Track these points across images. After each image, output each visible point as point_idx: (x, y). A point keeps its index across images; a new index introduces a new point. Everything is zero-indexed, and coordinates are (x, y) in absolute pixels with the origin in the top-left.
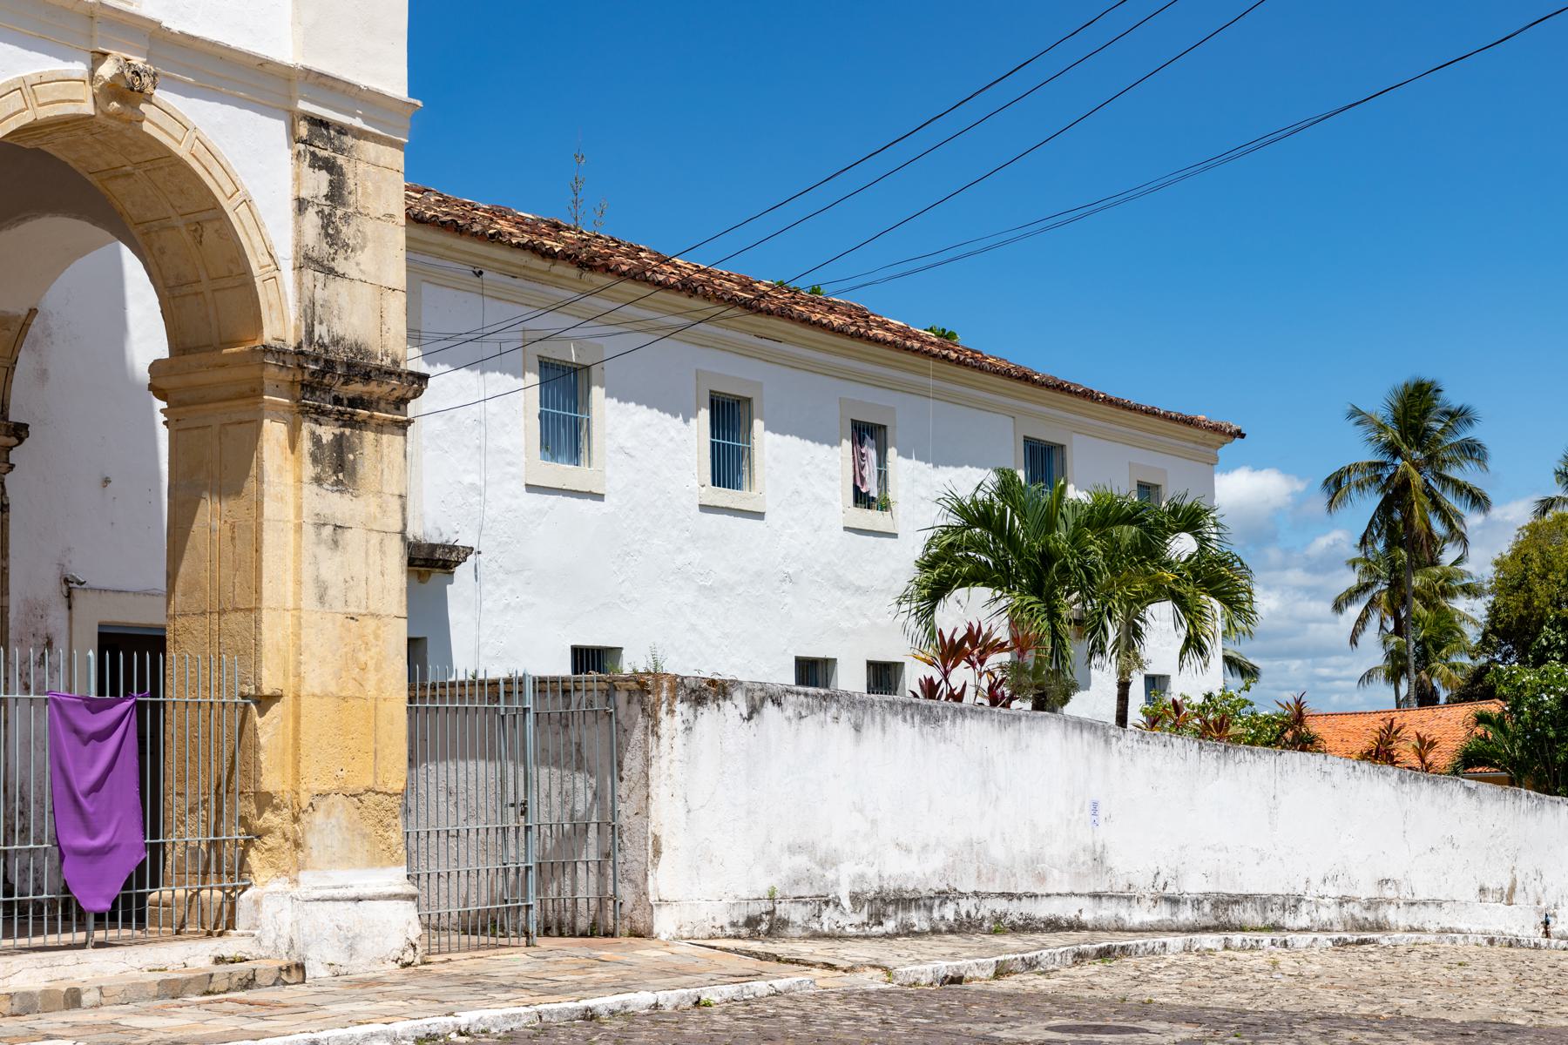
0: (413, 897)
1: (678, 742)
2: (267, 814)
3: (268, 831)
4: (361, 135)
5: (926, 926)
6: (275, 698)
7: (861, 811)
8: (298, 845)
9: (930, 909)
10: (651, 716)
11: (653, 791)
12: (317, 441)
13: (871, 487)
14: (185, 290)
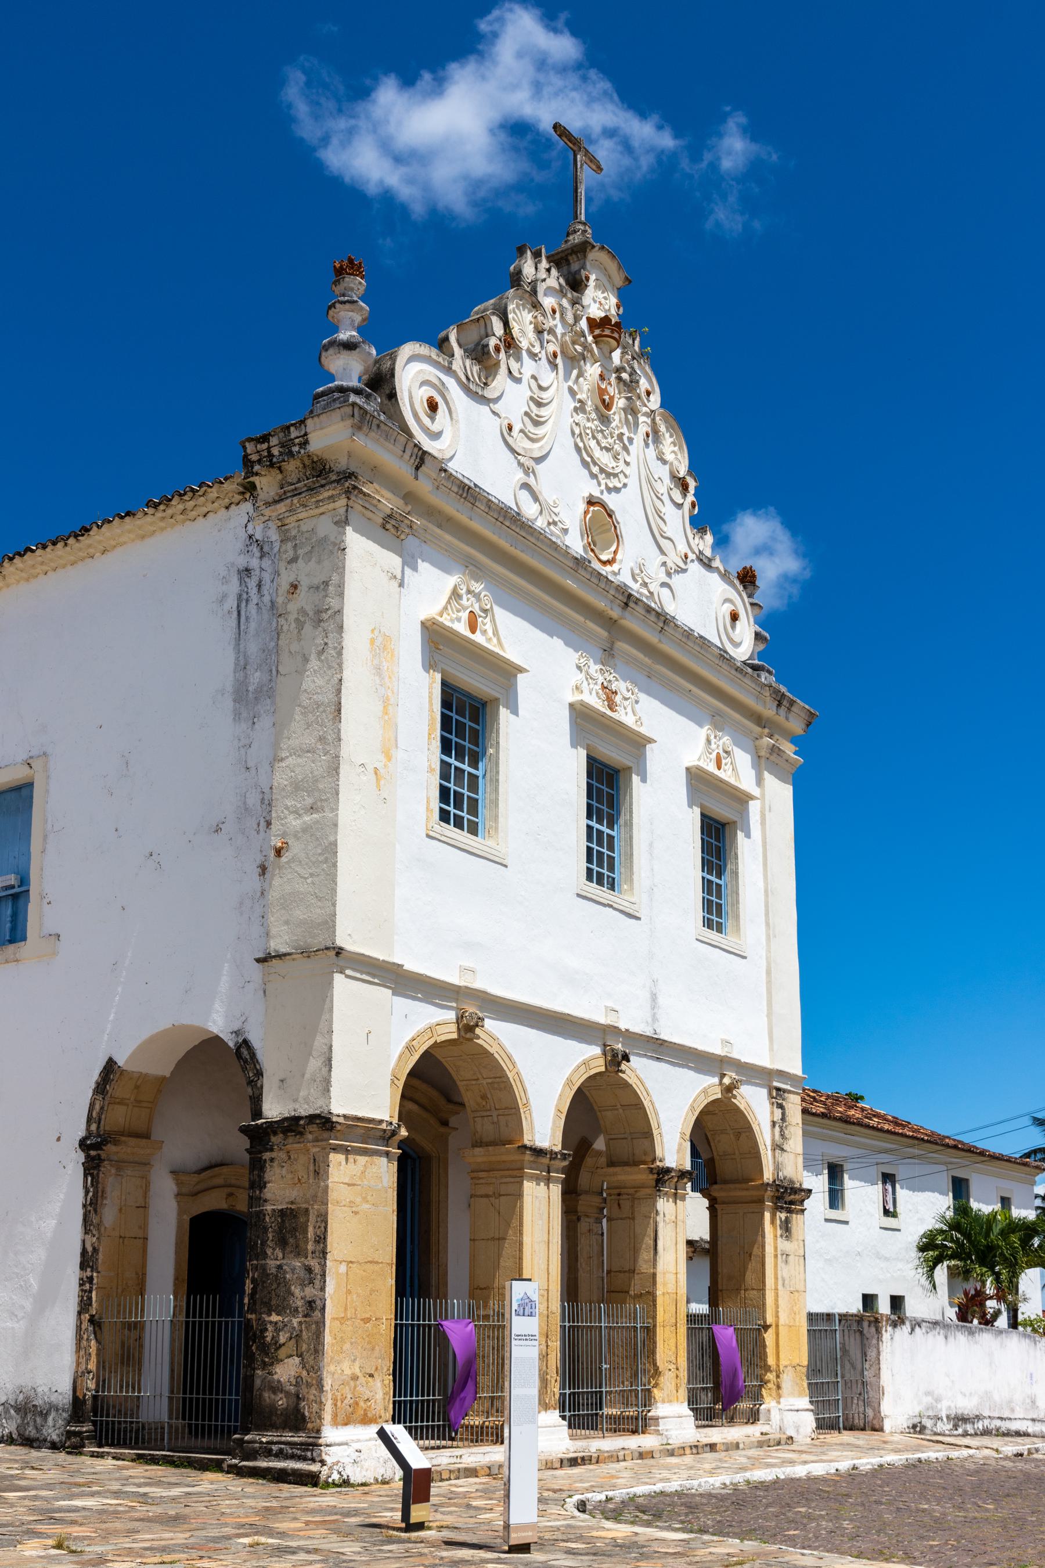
0: (812, 1411)
1: (889, 1344)
2: (768, 1374)
3: (769, 1381)
4: (790, 1092)
5: (972, 1432)
6: (770, 1326)
7: (948, 1376)
8: (779, 1387)
9: (974, 1423)
10: (878, 1331)
11: (881, 1366)
12: (781, 1219)
13: (890, 1207)
14: (727, 1157)
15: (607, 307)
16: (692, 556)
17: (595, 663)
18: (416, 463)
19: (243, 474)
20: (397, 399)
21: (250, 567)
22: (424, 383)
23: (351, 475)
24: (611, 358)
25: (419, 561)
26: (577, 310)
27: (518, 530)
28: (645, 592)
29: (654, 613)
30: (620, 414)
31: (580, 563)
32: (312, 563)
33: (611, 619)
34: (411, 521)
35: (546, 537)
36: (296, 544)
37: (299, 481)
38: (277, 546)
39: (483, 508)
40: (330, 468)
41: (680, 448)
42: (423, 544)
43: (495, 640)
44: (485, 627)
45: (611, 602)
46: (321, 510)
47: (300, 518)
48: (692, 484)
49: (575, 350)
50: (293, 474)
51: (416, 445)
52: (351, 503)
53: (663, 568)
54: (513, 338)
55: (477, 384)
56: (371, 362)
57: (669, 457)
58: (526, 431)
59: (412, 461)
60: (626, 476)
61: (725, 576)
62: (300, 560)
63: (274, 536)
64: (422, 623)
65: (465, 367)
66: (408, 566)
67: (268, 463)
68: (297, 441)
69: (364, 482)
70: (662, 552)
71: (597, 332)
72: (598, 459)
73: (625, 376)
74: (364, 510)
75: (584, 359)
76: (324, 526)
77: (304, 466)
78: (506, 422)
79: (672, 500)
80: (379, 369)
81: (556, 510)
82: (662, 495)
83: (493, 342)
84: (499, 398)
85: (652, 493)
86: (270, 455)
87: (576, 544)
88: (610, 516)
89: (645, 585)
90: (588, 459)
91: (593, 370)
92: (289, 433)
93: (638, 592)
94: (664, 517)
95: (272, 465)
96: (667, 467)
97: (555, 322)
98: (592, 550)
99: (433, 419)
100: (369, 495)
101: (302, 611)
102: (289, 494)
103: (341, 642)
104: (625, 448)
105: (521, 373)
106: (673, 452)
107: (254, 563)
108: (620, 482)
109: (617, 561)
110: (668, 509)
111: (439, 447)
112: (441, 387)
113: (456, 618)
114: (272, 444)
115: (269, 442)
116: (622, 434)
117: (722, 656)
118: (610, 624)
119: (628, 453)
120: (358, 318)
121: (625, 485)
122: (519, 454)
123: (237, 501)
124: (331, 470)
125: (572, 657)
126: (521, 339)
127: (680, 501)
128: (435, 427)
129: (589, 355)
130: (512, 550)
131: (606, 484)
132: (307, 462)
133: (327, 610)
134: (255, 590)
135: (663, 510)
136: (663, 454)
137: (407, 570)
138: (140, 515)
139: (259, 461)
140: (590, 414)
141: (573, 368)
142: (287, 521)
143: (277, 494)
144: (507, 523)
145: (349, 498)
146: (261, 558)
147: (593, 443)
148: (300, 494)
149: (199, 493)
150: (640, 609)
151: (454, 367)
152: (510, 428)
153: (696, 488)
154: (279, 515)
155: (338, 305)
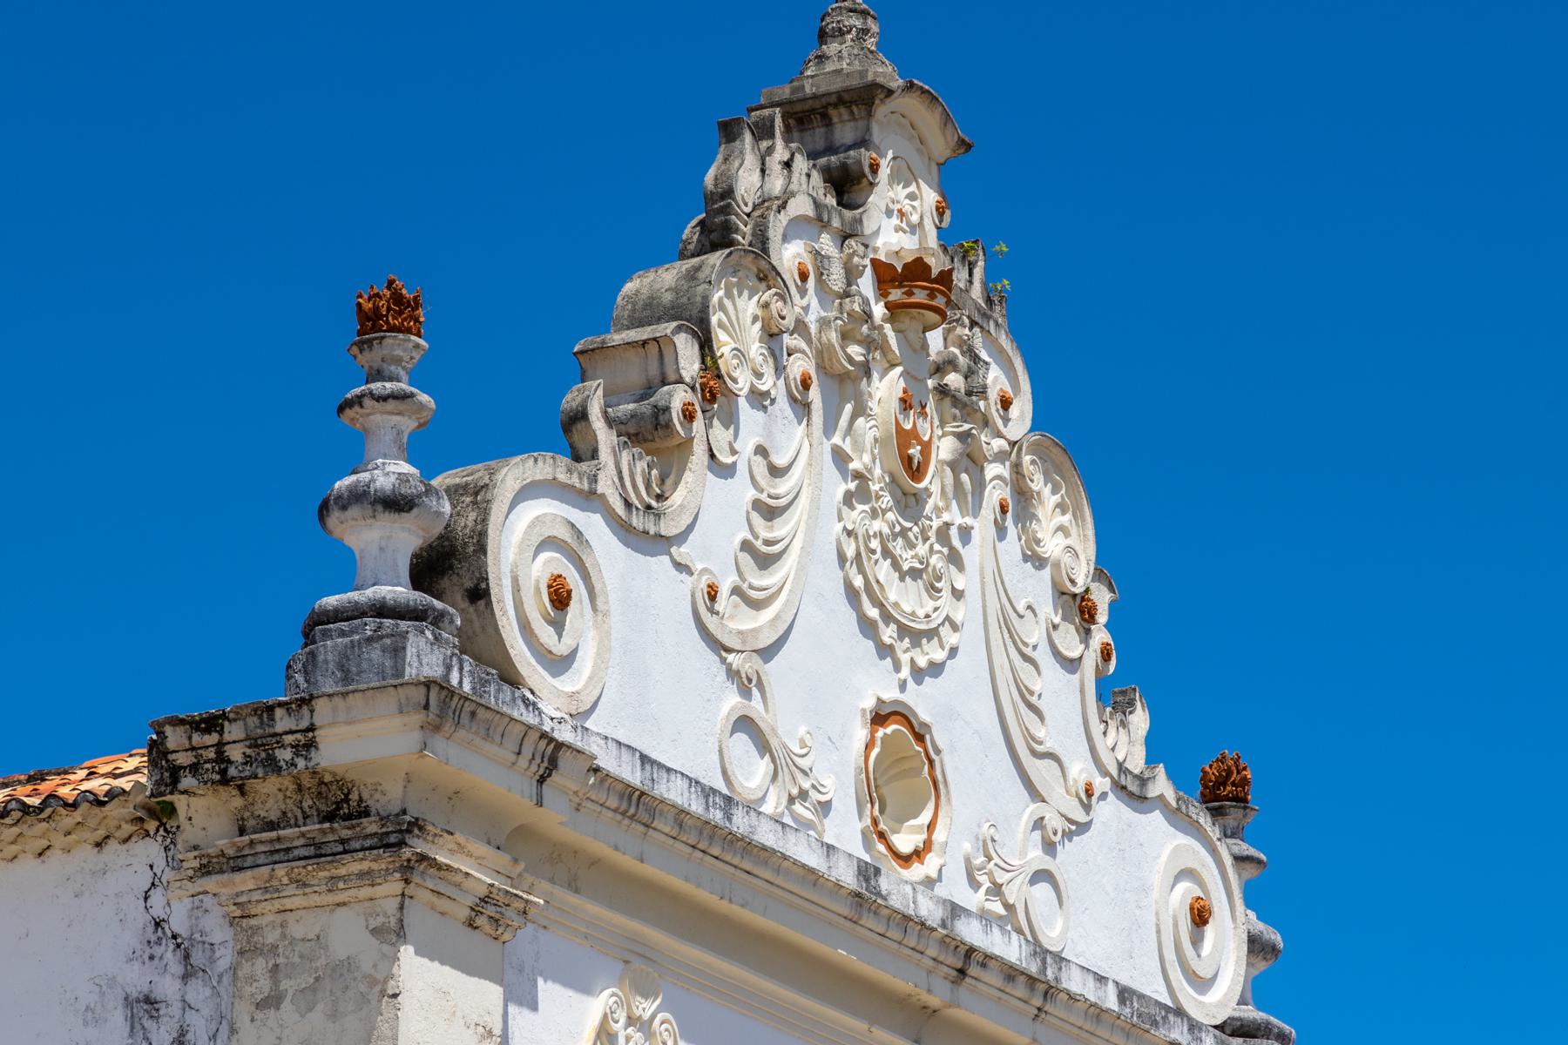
15: (915, 218)
18: (541, 772)
20: (489, 604)
21: (157, 994)
26: (851, 256)
29: (1022, 979)
32: (317, 1017)
33: (924, 1007)
34: (527, 901)
36: (276, 966)
38: (225, 958)
40: (361, 800)
42: (542, 931)
45: (929, 972)
46: (341, 897)
48: (1102, 598)
49: (850, 360)
53: (1037, 835)
54: (719, 376)
57: (1052, 546)
58: (745, 586)
60: (955, 627)
62: (286, 1004)
63: (218, 930)
65: (620, 473)
68: (289, 739)
69: (435, 835)
70: (1035, 794)
71: (896, 295)
72: (896, 605)
73: (954, 380)
75: (868, 374)
77: (300, 788)
79: (1056, 653)
81: (804, 763)
82: (1035, 647)
83: (679, 398)
85: (1012, 650)
86: (222, 759)
88: (920, 738)
90: (873, 613)
91: (886, 388)
94: (1041, 704)
96: (1046, 573)
97: (804, 302)
98: (882, 836)
99: (558, 626)
100: (449, 868)
104: (955, 559)
105: (734, 452)
106: (1061, 529)
107: (168, 987)
109: (935, 847)
111: (569, 689)
114: (227, 737)
121: (953, 652)
123: (126, 836)
127: (1074, 654)
128: (561, 648)
130: (723, 906)
131: (912, 661)
132: (307, 781)
135: (1037, 687)
136: (1038, 542)
140: (878, 498)
141: (844, 401)
143: (234, 844)
145: (407, 881)
146: (185, 977)
147: (884, 571)
150: (992, 977)
152: (712, 594)
153: (1112, 604)
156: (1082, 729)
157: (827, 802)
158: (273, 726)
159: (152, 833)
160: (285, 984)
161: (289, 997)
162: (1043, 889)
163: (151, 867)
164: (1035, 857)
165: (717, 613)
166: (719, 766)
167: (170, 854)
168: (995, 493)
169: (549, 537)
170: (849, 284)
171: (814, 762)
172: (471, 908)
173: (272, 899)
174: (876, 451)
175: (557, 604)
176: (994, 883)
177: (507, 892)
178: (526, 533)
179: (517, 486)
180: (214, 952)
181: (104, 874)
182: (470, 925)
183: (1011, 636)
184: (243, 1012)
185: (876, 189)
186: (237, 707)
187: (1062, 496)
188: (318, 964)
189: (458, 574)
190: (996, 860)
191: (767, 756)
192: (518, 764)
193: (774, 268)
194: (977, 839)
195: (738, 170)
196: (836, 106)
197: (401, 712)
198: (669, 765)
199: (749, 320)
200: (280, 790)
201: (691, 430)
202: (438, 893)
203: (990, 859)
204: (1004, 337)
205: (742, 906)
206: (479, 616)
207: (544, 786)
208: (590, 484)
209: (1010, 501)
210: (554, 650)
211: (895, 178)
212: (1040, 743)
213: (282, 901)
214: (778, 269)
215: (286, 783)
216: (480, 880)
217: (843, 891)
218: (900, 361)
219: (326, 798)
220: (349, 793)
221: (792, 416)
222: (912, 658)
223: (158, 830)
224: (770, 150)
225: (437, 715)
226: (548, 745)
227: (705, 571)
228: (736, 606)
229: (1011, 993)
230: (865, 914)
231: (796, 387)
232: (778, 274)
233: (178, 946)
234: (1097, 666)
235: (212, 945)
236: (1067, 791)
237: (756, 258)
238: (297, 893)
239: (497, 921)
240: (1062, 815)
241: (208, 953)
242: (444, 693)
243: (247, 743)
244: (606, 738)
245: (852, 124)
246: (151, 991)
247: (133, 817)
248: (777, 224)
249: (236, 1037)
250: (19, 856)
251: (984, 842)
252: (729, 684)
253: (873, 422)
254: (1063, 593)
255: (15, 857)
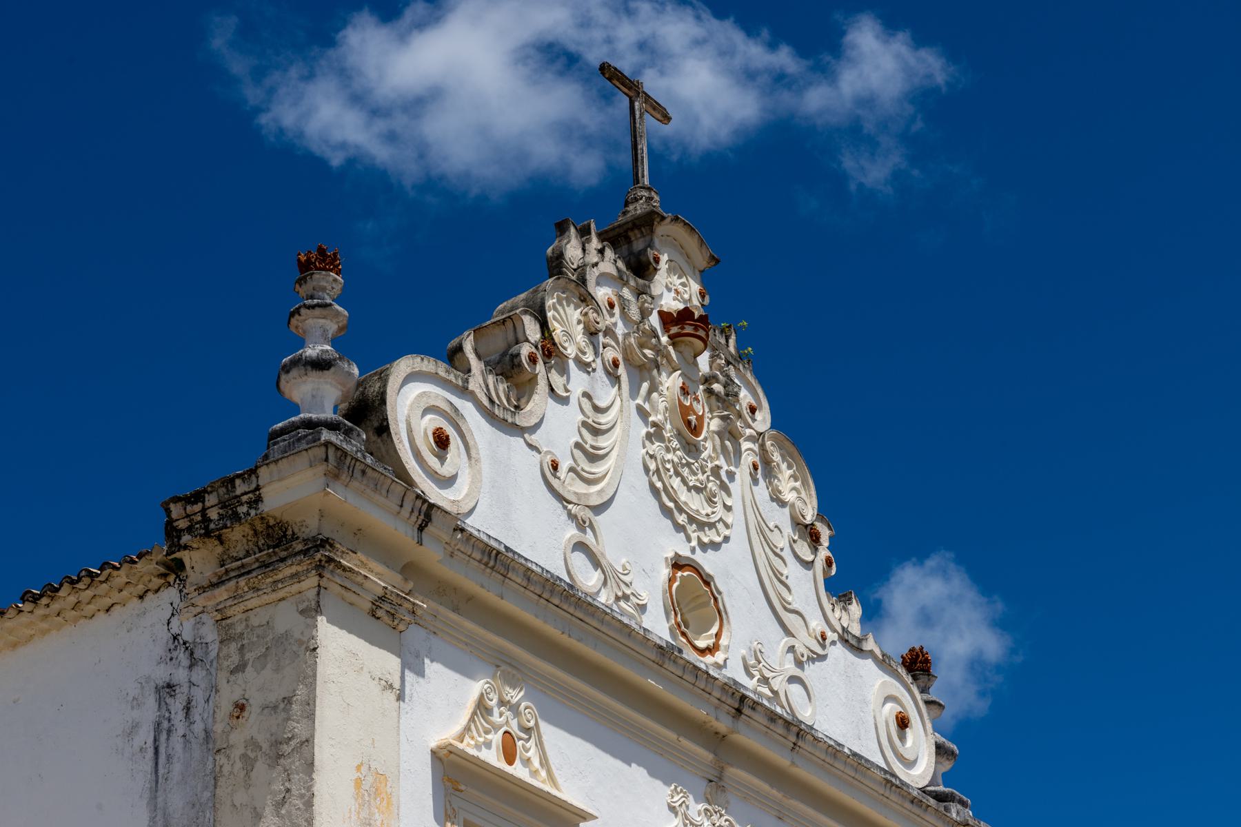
16: (831, 636)
17: (697, 802)
18: (419, 522)
19: (165, 548)
20: (389, 434)
22: (427, 411)
23: (325, 543)
24: (696, 364)
25: (427, 661)
27: (571, 610)
28: (766, 691)
29: (780, 721)
30: (713, 441)
31: (665, 653)
32: (267, 673)
33: (717, 733)
34: (414, 604)
35: (613, 618)
36: (243, 645)
37: (248, 554)
39: (519, 580)
40: (294, 533)
41: (804, 483)
42: (432, 636)
43: (543, 773)
44: (529, 754)
45: (716, 708)
46: (281, 594)
47: (249, 607)
48: (825, 533)
49: (645, 355)
50: (239, 545)
51: (418, 497)
52: (324, 583)
53: (790, 656)
55: (505, 408)
56: (352, 384)
57: (789, 496)
58: (579, 469)
59: (414, 518)
60: (727, 526)
61: (884, 663)
62: (249, 669)
63: (210, 634)
64: (433, 752)
65: (487, 386)
66: (410, 669)
67: (203, 531)
68: (245, 498)
69: (343, 552)
70: (788, 632)
71: (674, 330)
72: (686, 503)
73: (717, 387)
74: (343, 591)
75: (658, 367)
76: (285, 618)
77: (256, 533)
78: (548, 458)
80: (363, 393)
82: (782, 550)
84: (538, 426)
86: (206, 520)
87: (658, 625)
88: (707, 584)
89: (765, 681)
90: (671, 505)
91: (671, 382)
92: (234, 487)
93: (755, 692)
94: (788, 582)
95: (208, 534)
96: (787, 510)
98: (683, 634)
99: (442, 459)
100: (351, 570)
101: (253, 744)
102: (232, 574)
103: (311, 786)
104: (724, 487)
105: (567, 391)
106: (794, 489)
107: (181, 675)
108: (719, 535)
109: (722, 648)
110: (793, 571)
112: (453, 415)
113: (484, 743)
114: (207, 504)
115: (203, 502)
116: (718, 468)
117: (888, 781)
118: (716, 741)
119: (729, 494)
120: (332, 327)
121: (727, 539)
122: (570, 502)
123: (156, 588)
124: (295, 537)
125: (662, 793)
126: (566, 345)
127: (810, 558)
128: (446, 470)
129: (664, 362)
130: (565, 640)
131: (699, 538)
132: (260, 527)
133: (290, 739)
134: (181, 715)
135: (785, 572)
136: (780, 492)
137: (409, 676)
138: (11, 613)
139: (190, 530)
140: (670, 441)
142: (229, 613)
143: (216, 574)
144: (556, 601)
145: (321, 576)
146: (191, 667)
147: (676, 482)
148: (249, 572)
149: (101, 578)
150: (759, 717)
151: (472, 386)
152: (555, 466)
154: (218, 605)
155: (303, 311)
156: (817, 603)
157: (643, 605)
158: (234, 492)
159: (172, 584)
160: (248, 656)
161: (250, 663)
162: (796, 689)
163: (172, 604)
164: (790, 668)
165: (559, 478)
166: (564, 566)
167: (183, 594)
168: (748, 459)
169: (434, 406)
170: (643, 318)
171: (633, 579)
172: (372, 602)
173: (239, 603)
174: (667, 415)
175: (439, 444)
176: (763, 676)
177: (398, 595)
178: (415, 398)
179: (409, 370)
180: (207, 647)
181: (145, 614)
182: (373, 615)
183: (766, 540)
184: (222, 677)
185: (658, 272)
186: (212, 483)
187: (794, 471)
188: (268, 639)
189: (370, 420)
190: (763, 663)
191: (599, 570)
192: (401, 513)
193: (590, 294)
194: (751, 650)
195: (566, 245)
196: (632, 229)
197: (311, 466)
198: (526, 557)
199: (575, 322)
200: (244, 536)
201: (535, 369)
202: (345, 588)
203: (760, 662)
204: (750, 375)
205: (579, 641)
206: (384, 444)
207: (423, 533)
208: (463, 382)
209: (759, 463)
210: (438, 471)
211: (669, 271)
212: (790, 604)
213: (246, 603)
214: (593, 295)
215: (247, 530)
216: (376, 583)
217: (650, 642)
218: (680, 366)
219: (273, 537)
220: (286, 531)
221: (608, 382)
222: (698, 536)
223: (175, 581)
224: (589, 241)
225: (335, 467)
226: (423, 504)
227: (548, 452)
228: (573, 479)
229: (775, 730)
230: (667, 661)
231: (609, 365)
232: (593, 298)
233: (187, 648)
234: (824, 569)
235: (207, 643)
236: (809, 635)
237: (577, 286)
238: (253, 595)
239: (393, 615)
240: (807, 648)
241: (204, 649)
242: (339, 453)
243: (220, 506)
244: (479, 531)
245: (642, 239)
246: (171, 680)
247: (159, 573)
248: (592, 276)
249: (218, 694)
250: (96, 615)
251: (755, 651)
252: (570, 522)
253: (663, 399)
254: (799, 524)
255: (93, 616)
